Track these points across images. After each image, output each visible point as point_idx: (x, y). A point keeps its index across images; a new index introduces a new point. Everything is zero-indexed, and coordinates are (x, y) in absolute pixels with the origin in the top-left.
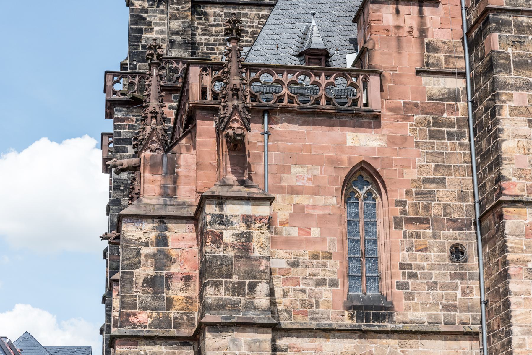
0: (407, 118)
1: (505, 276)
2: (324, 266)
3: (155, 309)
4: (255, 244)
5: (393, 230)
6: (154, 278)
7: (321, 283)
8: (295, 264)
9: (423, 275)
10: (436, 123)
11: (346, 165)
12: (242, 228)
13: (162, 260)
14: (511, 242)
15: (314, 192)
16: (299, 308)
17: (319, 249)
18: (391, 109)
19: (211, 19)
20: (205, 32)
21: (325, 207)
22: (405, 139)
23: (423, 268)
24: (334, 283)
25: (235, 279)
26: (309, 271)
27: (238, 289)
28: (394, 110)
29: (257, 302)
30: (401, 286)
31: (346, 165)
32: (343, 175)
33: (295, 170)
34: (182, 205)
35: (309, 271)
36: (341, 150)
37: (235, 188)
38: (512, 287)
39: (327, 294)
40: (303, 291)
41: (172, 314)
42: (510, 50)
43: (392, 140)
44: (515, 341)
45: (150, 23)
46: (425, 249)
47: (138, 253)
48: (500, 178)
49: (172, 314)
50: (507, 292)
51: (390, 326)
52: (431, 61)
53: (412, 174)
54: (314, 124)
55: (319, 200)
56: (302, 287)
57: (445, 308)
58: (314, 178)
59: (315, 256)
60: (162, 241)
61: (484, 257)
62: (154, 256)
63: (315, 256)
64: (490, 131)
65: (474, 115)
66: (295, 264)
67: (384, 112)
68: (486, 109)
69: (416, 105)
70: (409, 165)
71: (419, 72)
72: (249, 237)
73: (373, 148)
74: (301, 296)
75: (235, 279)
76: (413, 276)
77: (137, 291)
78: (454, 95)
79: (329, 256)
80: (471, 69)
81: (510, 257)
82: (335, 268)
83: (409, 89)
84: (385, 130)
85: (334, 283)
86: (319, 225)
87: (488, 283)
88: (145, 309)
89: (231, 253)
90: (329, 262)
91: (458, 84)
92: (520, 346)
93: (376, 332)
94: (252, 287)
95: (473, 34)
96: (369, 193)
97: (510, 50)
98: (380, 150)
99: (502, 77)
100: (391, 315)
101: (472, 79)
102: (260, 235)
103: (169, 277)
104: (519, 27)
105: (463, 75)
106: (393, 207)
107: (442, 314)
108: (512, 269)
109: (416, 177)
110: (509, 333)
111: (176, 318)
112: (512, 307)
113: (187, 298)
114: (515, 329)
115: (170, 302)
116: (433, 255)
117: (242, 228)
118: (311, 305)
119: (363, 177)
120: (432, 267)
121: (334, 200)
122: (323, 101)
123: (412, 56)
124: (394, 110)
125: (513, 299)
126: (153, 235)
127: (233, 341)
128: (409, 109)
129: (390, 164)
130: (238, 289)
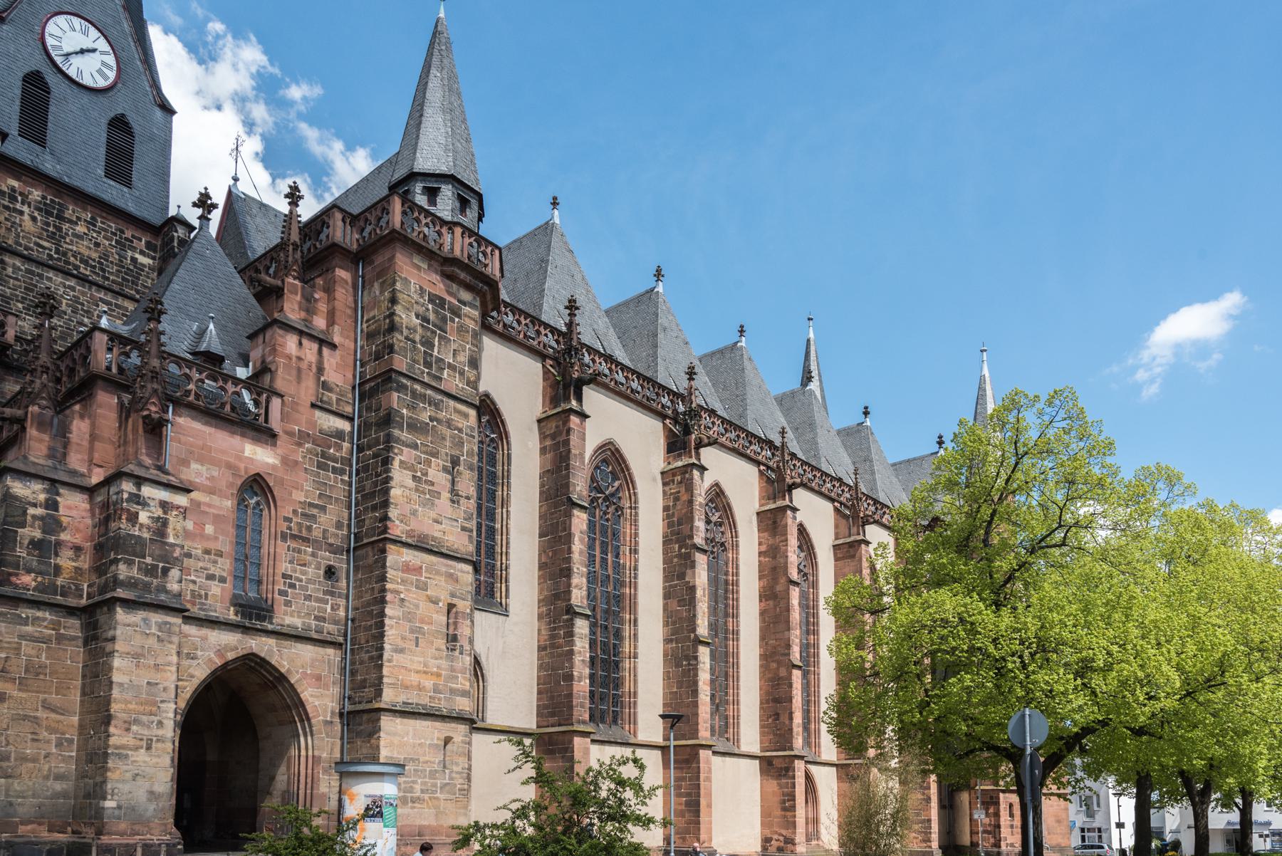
0: (300, 445)
1: (382, 601)
2: (215, 562)
3: (40, 573)
5: (279, 542)
6: (41, 541)
7: (211, 577)
9: (301, 588)
10: (324, 455)
11: (243, 473)
13: (52, 524)
14: (391, 574)
15: (211, 491)
16: (188, 598)
17: (212, 545)
18: (287, 433)
21: (220, 508)
22: (296, 463)
23: (301, 581)
24: (222, 580)
25: (149, 560)
26: (201, 564)
27: (151, 571)
28: (290, 434)
29: (169, 586)
30: (282, 593)
31: (243, 473)
32: (239, 483)
34: (74, 473)
35: (201, 564)
37: (152, 471)
38: (388, 611)
39: (215, 589)
40: (194, 582)
42: (405, 411)
43: (285, 460)
44: (386, 656)
46: (304, 565)
48: (385, 518)
49: (60, 581)
50: (382, 614)
51: (270, 627)
52: (325, 398)
53: (299, 496)
54: (216, 427)
55: (215, 500)
56: (193, 578)
57: (317, 618)
58: (211, 478)
59: (207, 552)
61: (355, 581)
62: (42, 518)
63: (207, 552)
64: (377, 475)
65: (358, 458)
67: (281, 433)
68: (375, 456)
69: (308, 435)
70: (298, 487)
71: (313, 406)
72: (165, 523)
73: (267, 464)
74: (191, 586)
76: (292, 586)
78: (339, 435)
80: (360, 417)
81: (388, 586)
82: (224, 566)
83: (303, 419)
84: (279, 451)
85: (222, 580)
87: (358, 603)
90: (219, 559)
91: (345, 426)
92: (389, 661)
93: (258, 630)
94: (165, 571)
95: (367, 387)
96: (258, 503)
97: (405, 411)
98: (274, 467)
99: (396, 432)
100: (271, 618)
101: (359, 426)
104: (414, 392)
105: (351, 419)
106: (280, 522)
107: (314, 623)
108: (389, 597)
109: (303, 499)
110: (382, 649)
111: (63, 587)
112: (386, 628)
113: (76, 568)
114: (387, 646)
115: (58, 570)
116: (310, 570)
118: (200, 596)
119: (257, 486)
120: (309, 581)
121: (229, 504)
122: (228, 408)
123: (307, 391)
124: (290, 434)
125: (387, 621)
126: (42, 497)
127: (144, 620)
128: (303, 437)
129: (281, 482)
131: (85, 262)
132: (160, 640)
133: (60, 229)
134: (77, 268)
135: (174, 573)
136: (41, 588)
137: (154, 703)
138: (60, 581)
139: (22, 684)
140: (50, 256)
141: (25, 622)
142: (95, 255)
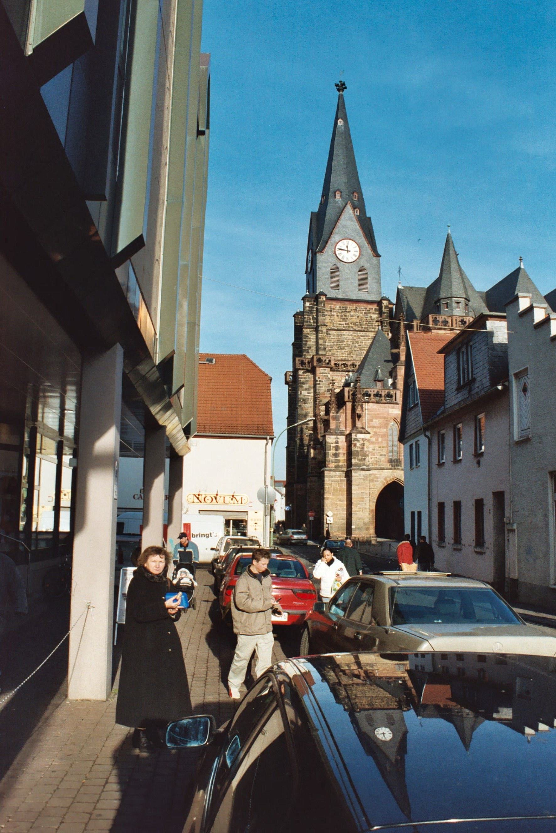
3: (335, 462)
4: (365, 447)
7: (381, 455)
8: (374, 449)
12: (362, 442)
15: (380, 427)
19: (332, 336)
20: (330, 341)
24: (385, 455)
25: (360, 457)
27: (361, 460)
33: (374, 420)
36: (388, 414)
41: (340, 464)
45: (310, 338)
47: (330, 446)
60: (337, 442)
63: (380, 447)
66: (374, 449)
72: (363, 445)
75: (360, 457)
77: (330, 457)
79: (383, 447)
86: (381, 437)
88: (332, 462)
89: (359, 450)
94: (365, 459)
102: (366, 443)
103: (339, 453)
117: (362, 442)
130: (361, 460)
131: (355, 324)
132: (364, 480)
133: (345, 316)
134: (352, 327)
135: (367, 459)
136: (336, 467)
137: (363, 498)
138: (340, 464)
139: (333, 494)
140: (344, 327)
141: (332, 477)
142: (358, 321)
